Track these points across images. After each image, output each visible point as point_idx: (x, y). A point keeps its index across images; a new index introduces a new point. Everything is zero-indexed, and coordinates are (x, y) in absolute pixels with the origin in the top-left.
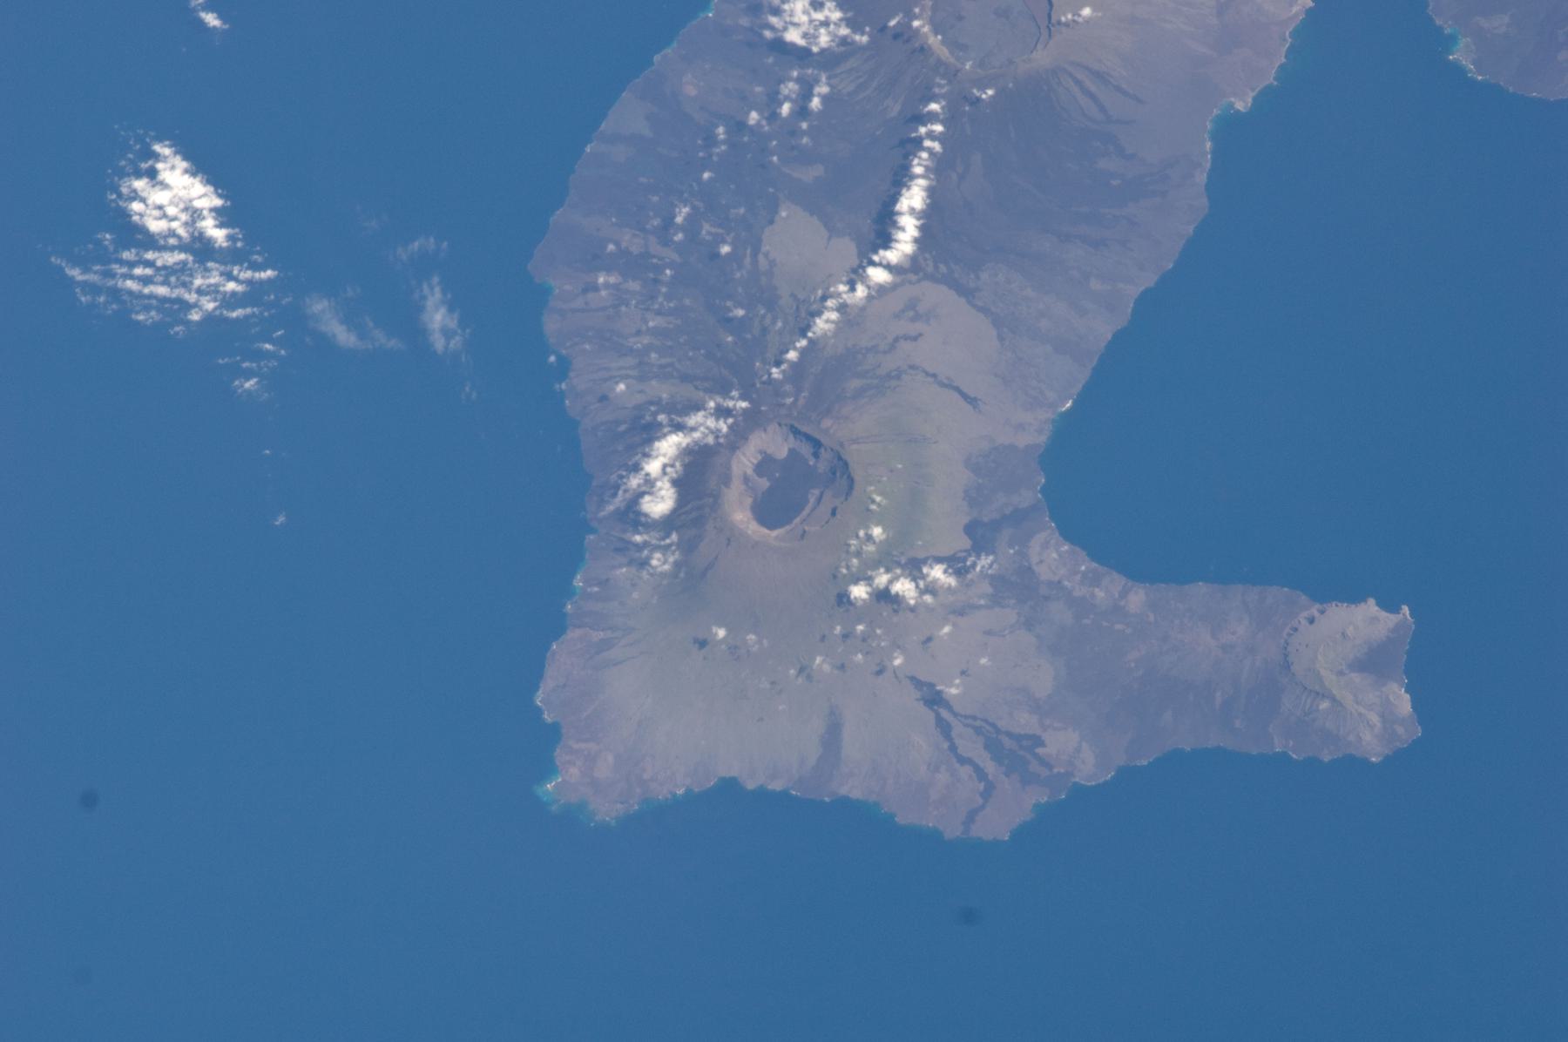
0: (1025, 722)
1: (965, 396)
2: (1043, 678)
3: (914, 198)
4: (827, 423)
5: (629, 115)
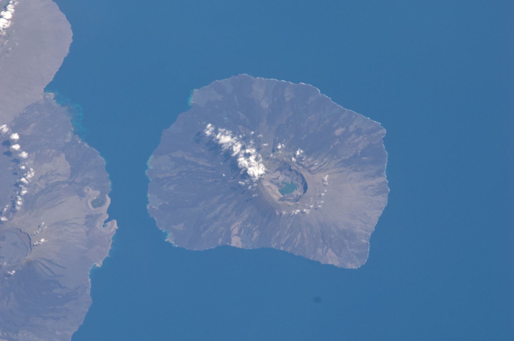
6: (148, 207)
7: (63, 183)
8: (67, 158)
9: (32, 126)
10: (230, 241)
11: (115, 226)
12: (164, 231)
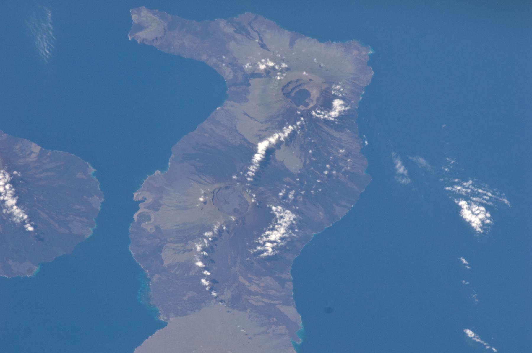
0: (238, 37)
1: (247, 115)
2: (232, 45)
3: (258, 157)
4: (288, 106)
5: (341, 212)
6: (103, 200)
7: (171, 242)
8: (162, 262)
9: (186, 298)
10: (41, 151)
11: (135, 195)
12: (95, 177)
